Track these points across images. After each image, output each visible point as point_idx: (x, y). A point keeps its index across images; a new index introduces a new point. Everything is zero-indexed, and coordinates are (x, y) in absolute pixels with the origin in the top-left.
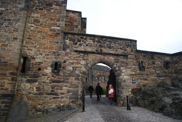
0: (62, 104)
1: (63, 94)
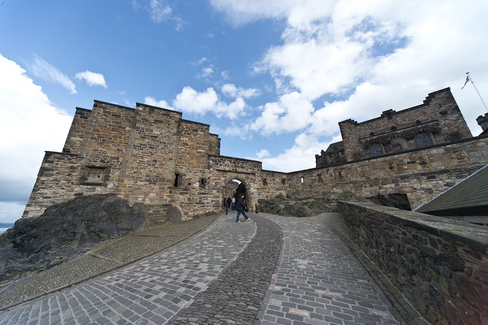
0: (207, 211)
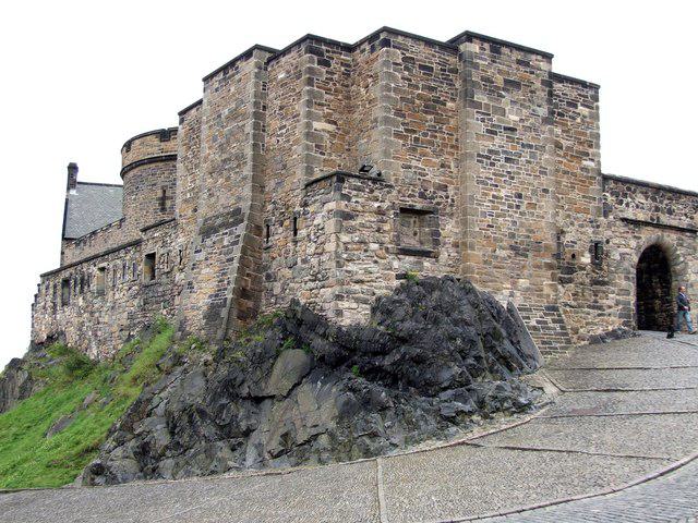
0: (610, 328)
1: (610, 307)
